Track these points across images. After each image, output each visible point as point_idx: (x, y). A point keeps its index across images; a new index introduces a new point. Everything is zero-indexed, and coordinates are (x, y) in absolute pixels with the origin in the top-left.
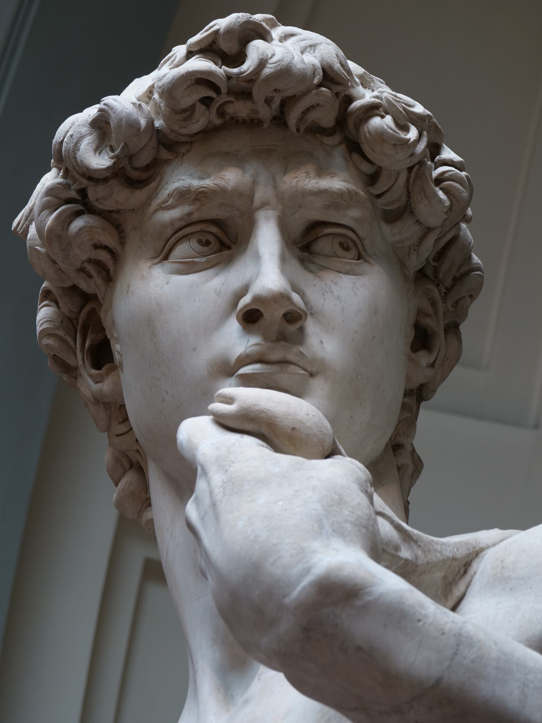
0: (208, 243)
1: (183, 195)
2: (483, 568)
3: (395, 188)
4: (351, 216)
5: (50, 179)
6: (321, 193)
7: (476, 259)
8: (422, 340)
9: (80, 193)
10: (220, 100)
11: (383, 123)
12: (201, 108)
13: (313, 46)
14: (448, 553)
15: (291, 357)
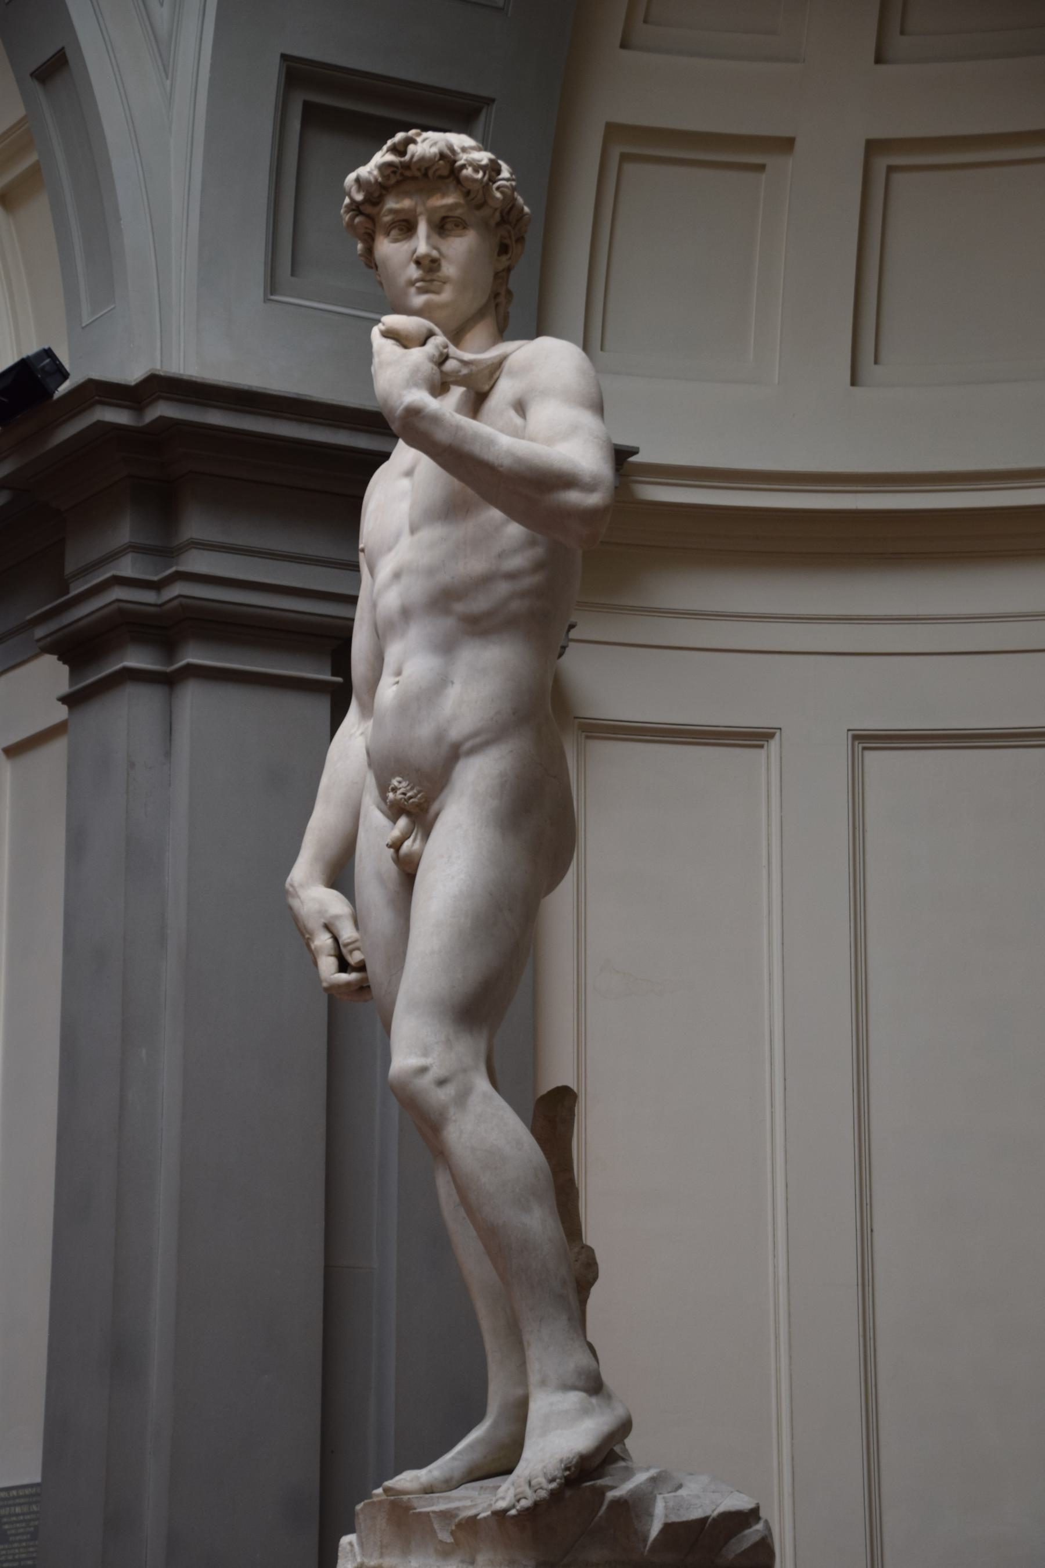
0: (401, 230)
1: (392, 211)
2: (507, 365)
3: (476, 196)
4: (458, 212)
5: (347, 200)
6: (443, 206)
7: (526, 209)
8: (503, 249)
9: (356, 208)
10: (399, 172)
11: (468, 172)
12: (392, 175)
13: (435, 144)
14: (489, 362)
15: (434, 277)
